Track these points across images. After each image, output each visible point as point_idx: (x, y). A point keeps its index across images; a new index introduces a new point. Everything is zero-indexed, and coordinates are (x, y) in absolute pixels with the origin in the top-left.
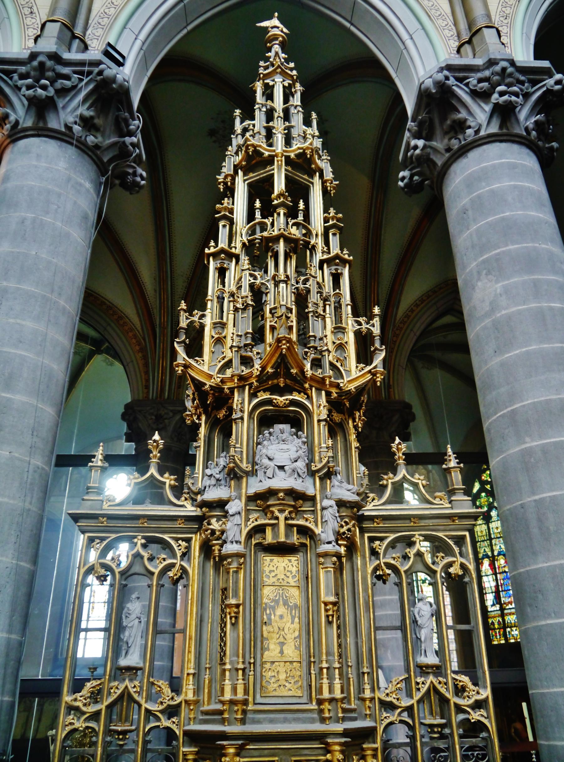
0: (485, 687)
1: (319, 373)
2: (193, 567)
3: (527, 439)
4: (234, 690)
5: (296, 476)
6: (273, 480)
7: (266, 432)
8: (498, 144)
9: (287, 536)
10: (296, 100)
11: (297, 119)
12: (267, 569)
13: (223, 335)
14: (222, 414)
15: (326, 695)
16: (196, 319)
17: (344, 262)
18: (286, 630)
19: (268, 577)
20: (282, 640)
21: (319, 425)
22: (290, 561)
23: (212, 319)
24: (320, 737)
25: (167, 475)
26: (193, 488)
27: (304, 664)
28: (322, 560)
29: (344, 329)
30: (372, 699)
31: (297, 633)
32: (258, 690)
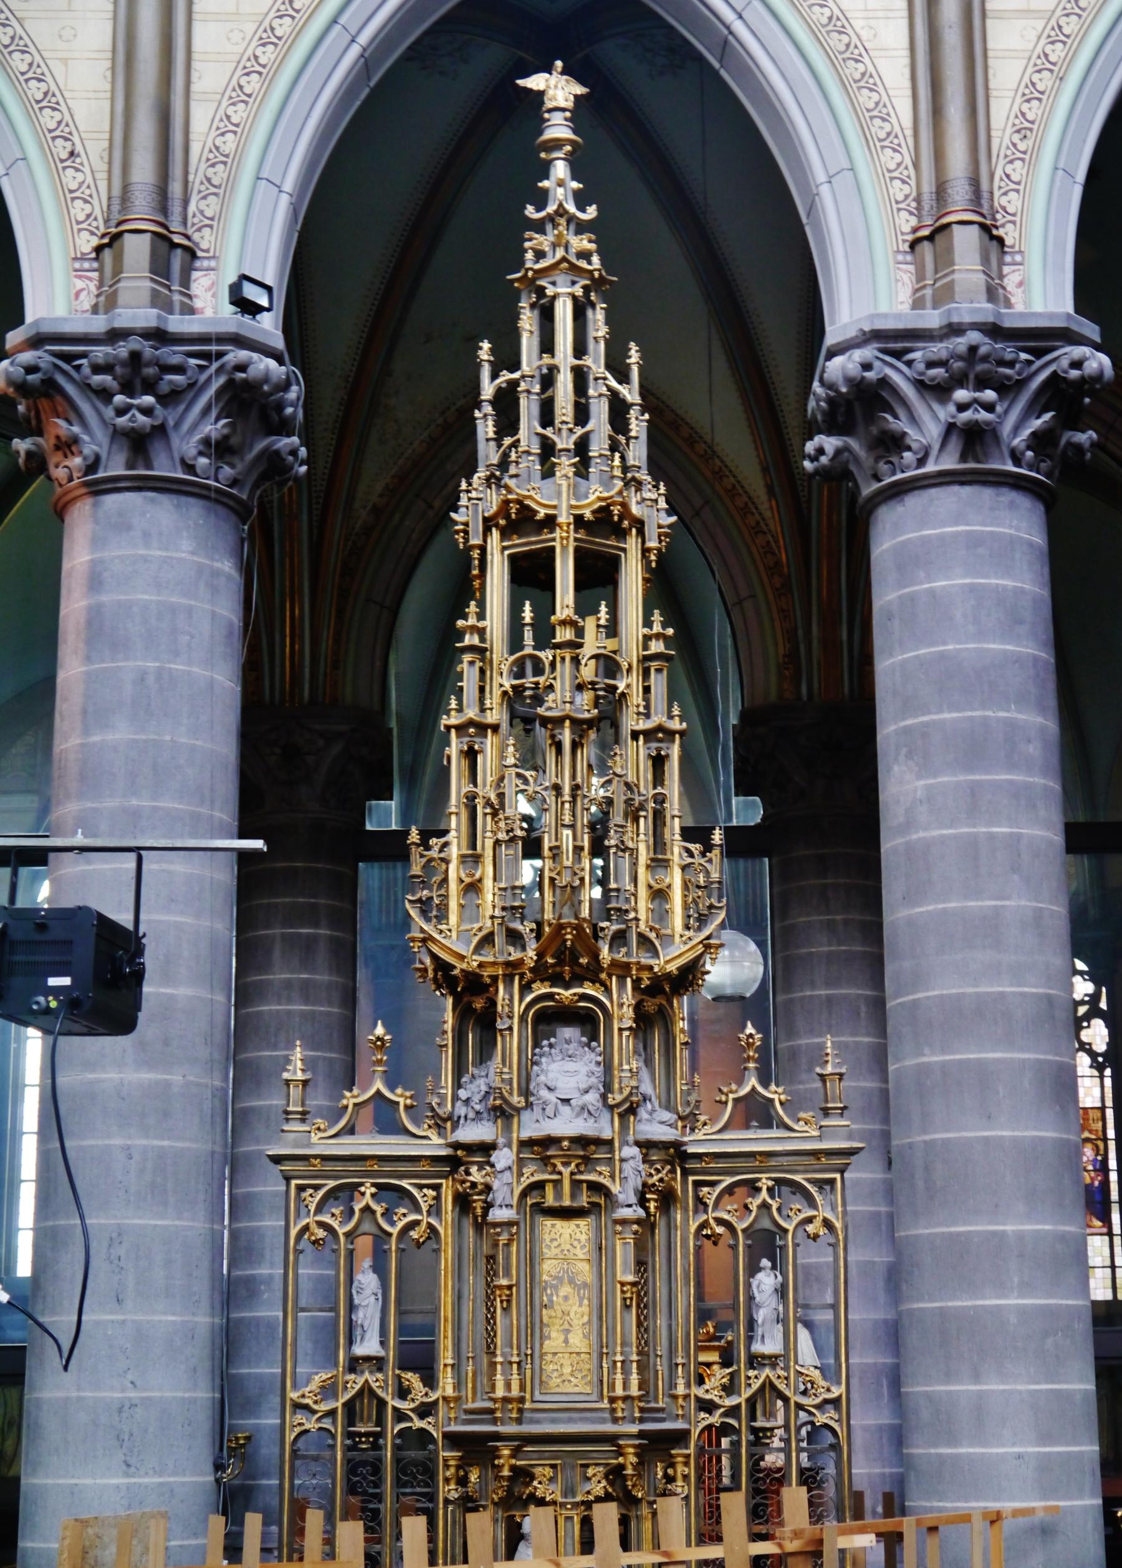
0: (839, 1383)
1: (620, 956)
2: (445, 1227)
3: (927, 1050)
4: (508, 1386)
5: (586, 1115)
6: (556, 1121)
7: (545, 1042)
8: (956, 488)
9: (573, 1196)
10: (598, 323)
12: (547, 1237)
13: (477, 876)
14: (479, 1004)
15: (619, 1392)
16: (434, 853)
17: (670, 734)
18: (572, 1315)
19: (549, 1247)
20: (566, 1326)
21: (620, 1035)
22: (578, 1226)
23: (459, 848)
24: (611, 1439)
25: (399, 1091)
26: (440, 1111)
27: (595, 1355)
28: (619, 1228)
29: (668, 861)
30: (686, 1397)
31: (586, 1319)
32: (537, 1386)
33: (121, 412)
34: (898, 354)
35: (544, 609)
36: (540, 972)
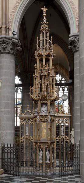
1: (49, 98)
10: (48, 35)
11: (48, 39)
33: (2, 46)
34: (76, 37)
35: (42, 64)
36: (41, 100)
